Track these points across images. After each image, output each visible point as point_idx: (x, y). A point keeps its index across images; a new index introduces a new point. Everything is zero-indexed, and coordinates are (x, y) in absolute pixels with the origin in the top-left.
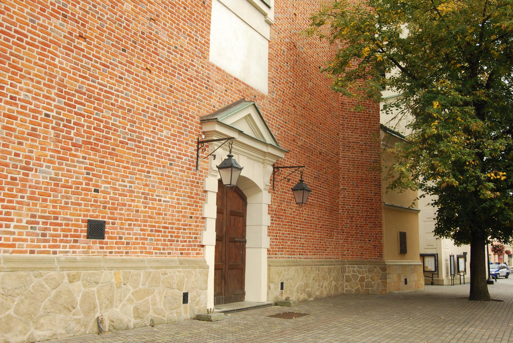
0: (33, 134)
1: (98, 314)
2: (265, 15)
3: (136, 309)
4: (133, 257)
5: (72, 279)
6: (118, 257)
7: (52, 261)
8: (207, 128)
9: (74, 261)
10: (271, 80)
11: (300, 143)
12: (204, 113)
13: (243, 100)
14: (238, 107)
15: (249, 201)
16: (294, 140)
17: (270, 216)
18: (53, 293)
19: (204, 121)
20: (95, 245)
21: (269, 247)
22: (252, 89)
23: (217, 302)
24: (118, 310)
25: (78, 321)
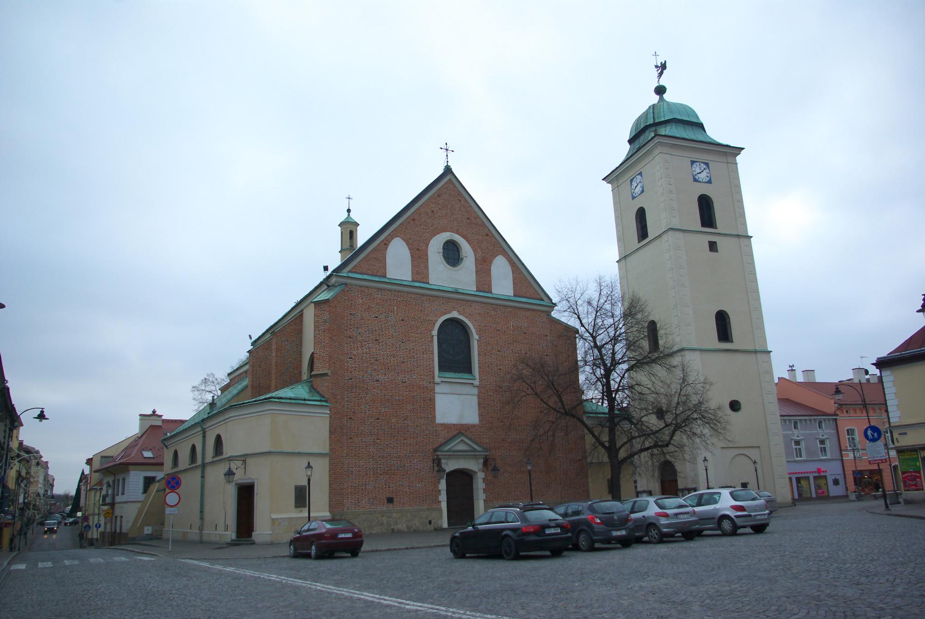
0: (366, 474)
1: (392, 527)
2: (473, 384)
3: (407, 526)
4: (405, 508)
5: (382, 516)
6: (399, 508)
7: (375, 511)
8: (436, 454)
9: (383, 511)
10: (480, 415)
11: (509, 440)
12: (435, 446)
13: (460, 433)
14: (456, 438)
15: (474, 477)
16: (503, 440)
17: (484, 484)
18: (377, 521)
19: (435, 450)
20: (391, 505)
21: (485, 498)
22: (466, 425)
23: (449, 524)
24: (400, 526)
25: (385, 529)
